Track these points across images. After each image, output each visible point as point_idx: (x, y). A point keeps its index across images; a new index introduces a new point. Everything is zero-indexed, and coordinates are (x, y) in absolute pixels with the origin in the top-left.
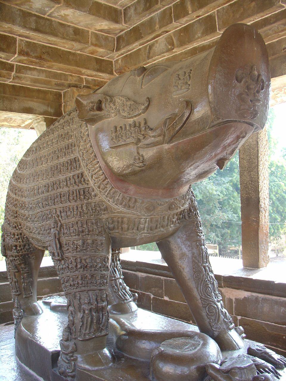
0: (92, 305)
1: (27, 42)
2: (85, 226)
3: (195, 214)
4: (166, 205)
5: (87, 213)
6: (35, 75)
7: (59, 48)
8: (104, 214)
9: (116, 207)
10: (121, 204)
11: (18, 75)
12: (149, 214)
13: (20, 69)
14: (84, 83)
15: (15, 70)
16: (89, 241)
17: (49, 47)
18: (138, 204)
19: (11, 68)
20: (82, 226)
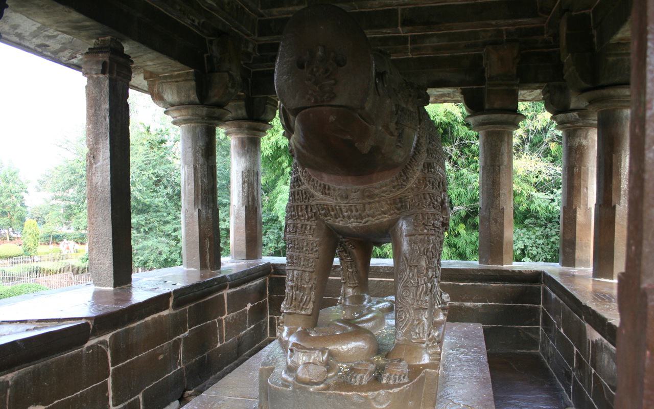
0: (293, 282)
1: (410, 9)
2: (296, 211)
3: (419, 205)
4: (358, 193)
5: (298, 199)
6: (434, 42)
7: (451, 3)
8: (313, 200)
9: (316, 193)
10: (320, 191)
11: (415, 46)
12: (345, 202)
13: (414, 40)
14: (505, 37)
15: (409, 42)
16: (299, 225)
17: (439, 6)
18: (332, 191)
19: (404, 40)
20: (294, 211)
